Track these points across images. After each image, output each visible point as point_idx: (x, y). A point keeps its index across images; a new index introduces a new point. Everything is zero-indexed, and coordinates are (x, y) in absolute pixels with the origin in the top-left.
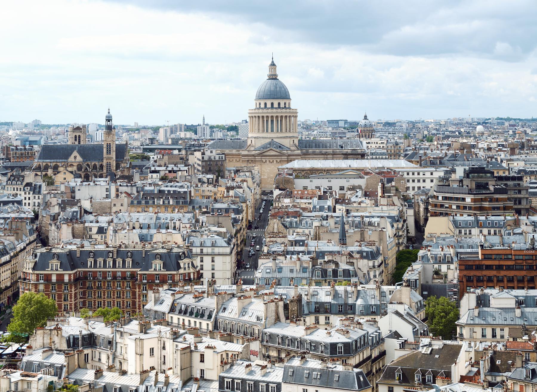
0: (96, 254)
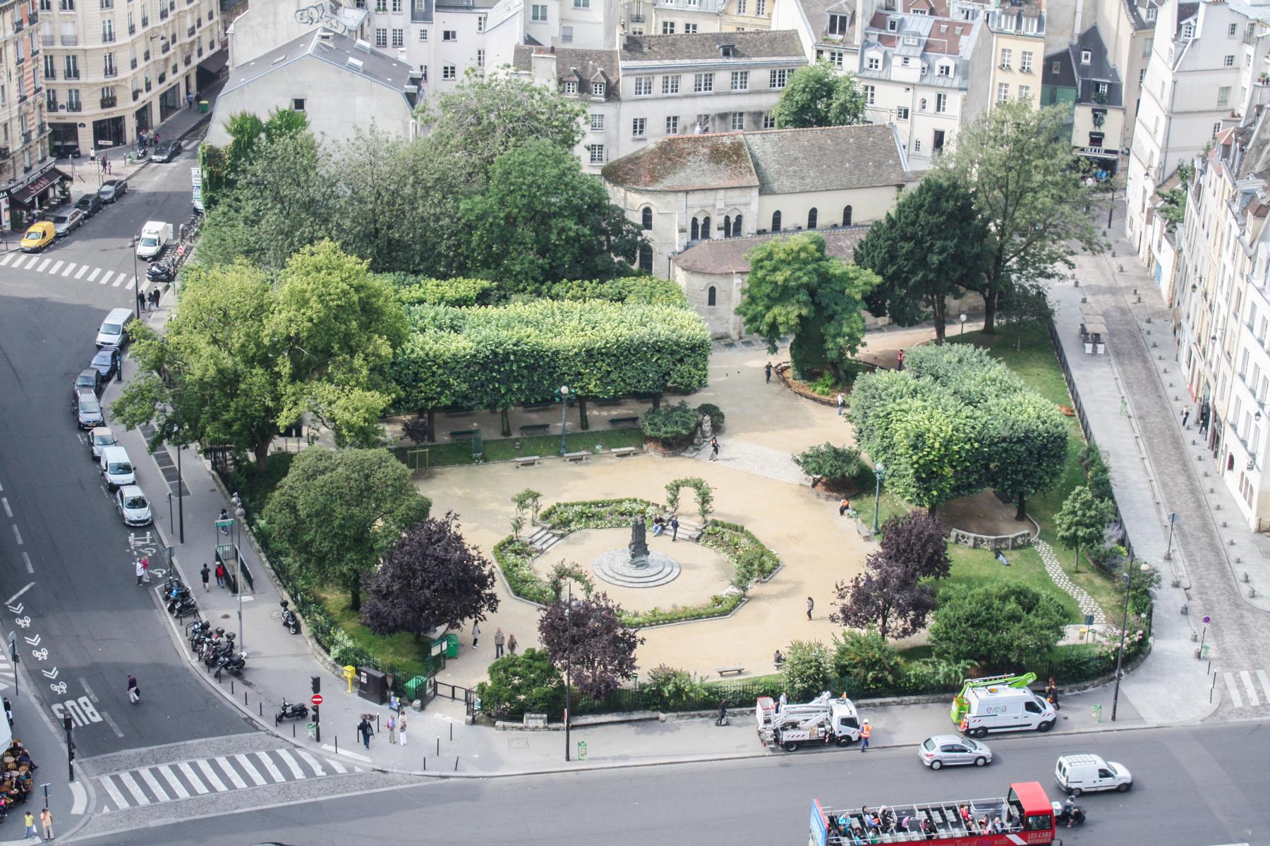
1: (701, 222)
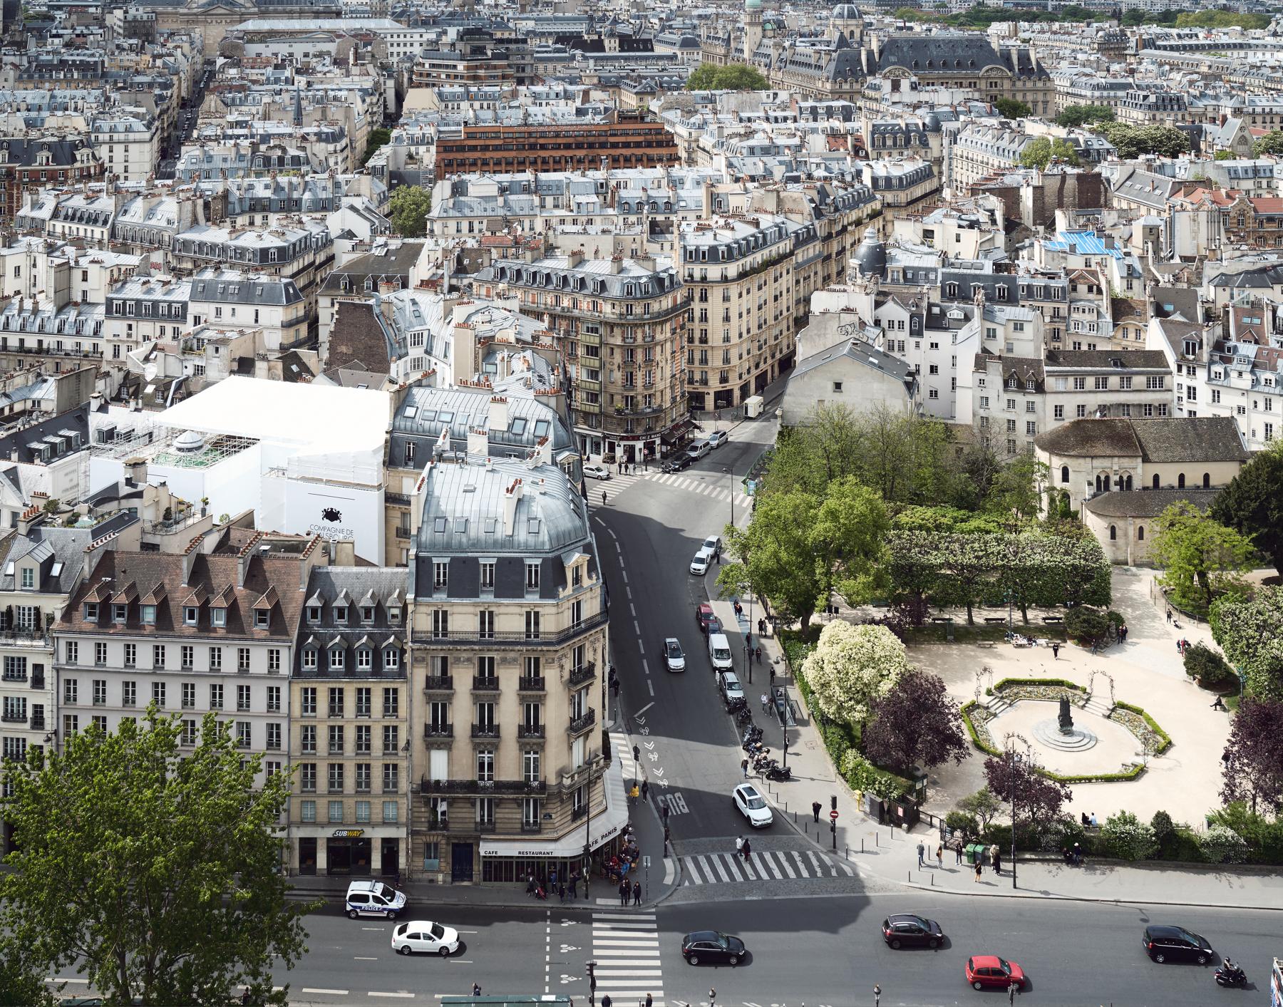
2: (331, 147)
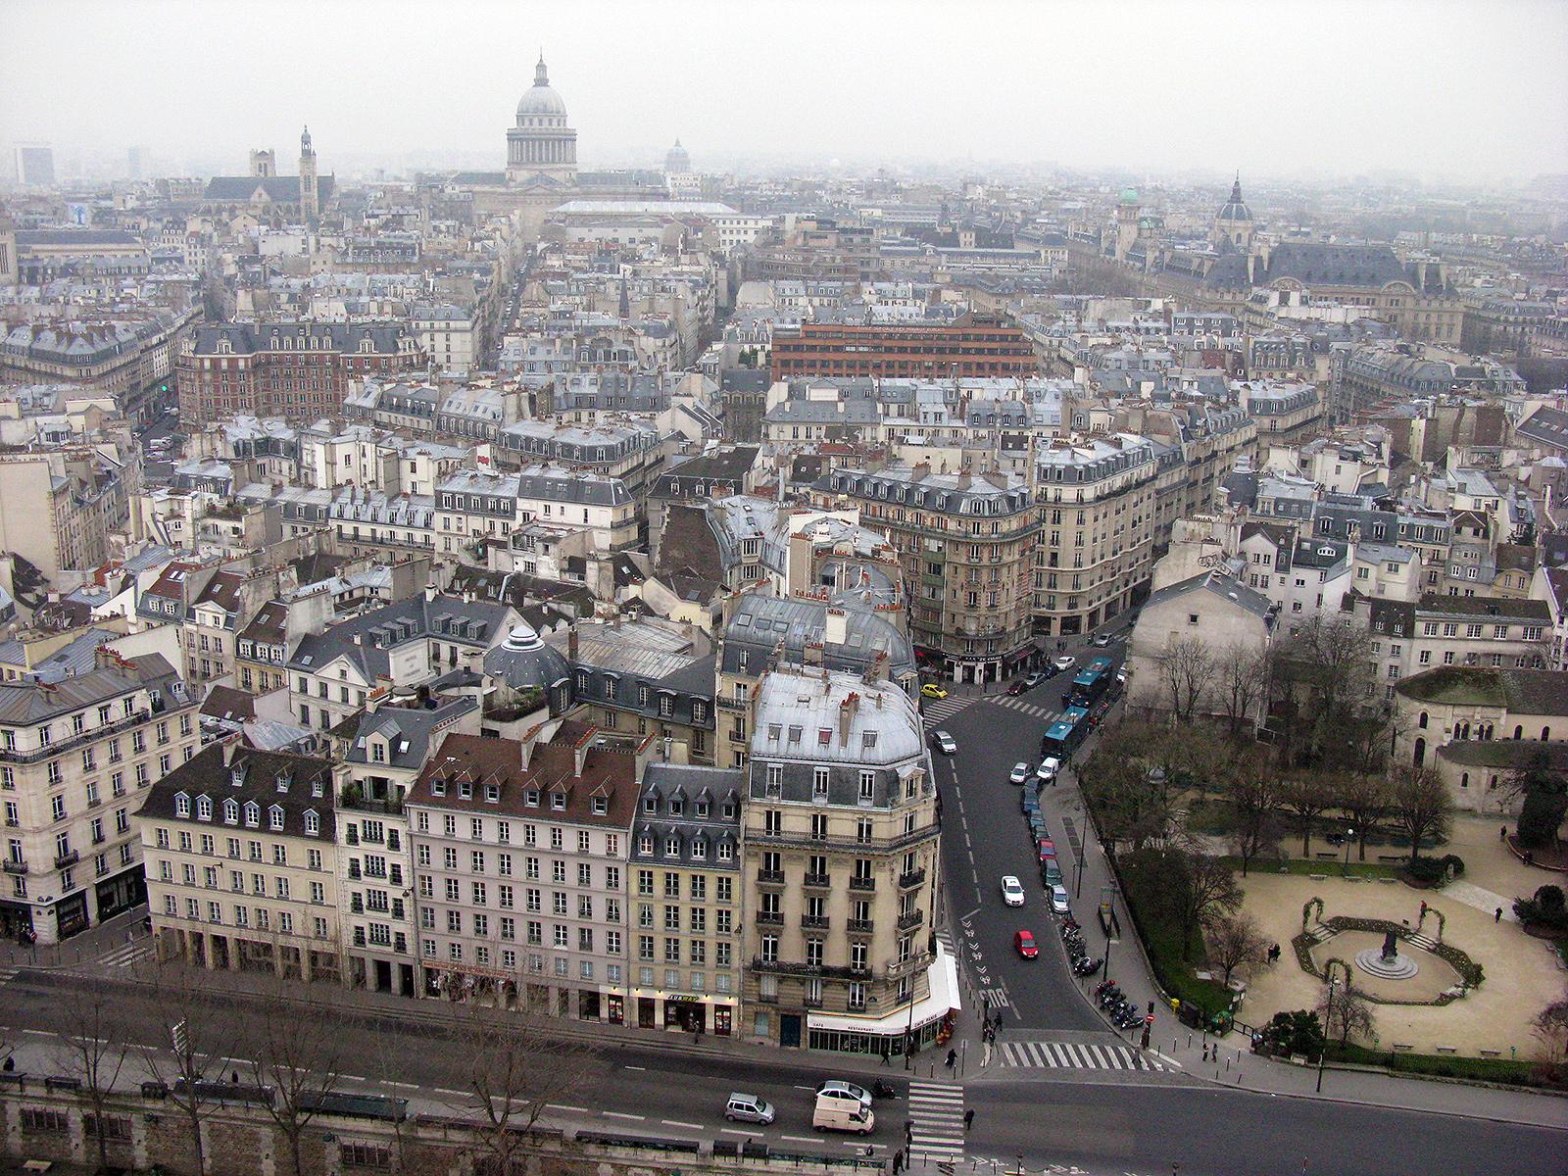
0: (282, 330)
1: (1462, 726)
2: (659, 342)
